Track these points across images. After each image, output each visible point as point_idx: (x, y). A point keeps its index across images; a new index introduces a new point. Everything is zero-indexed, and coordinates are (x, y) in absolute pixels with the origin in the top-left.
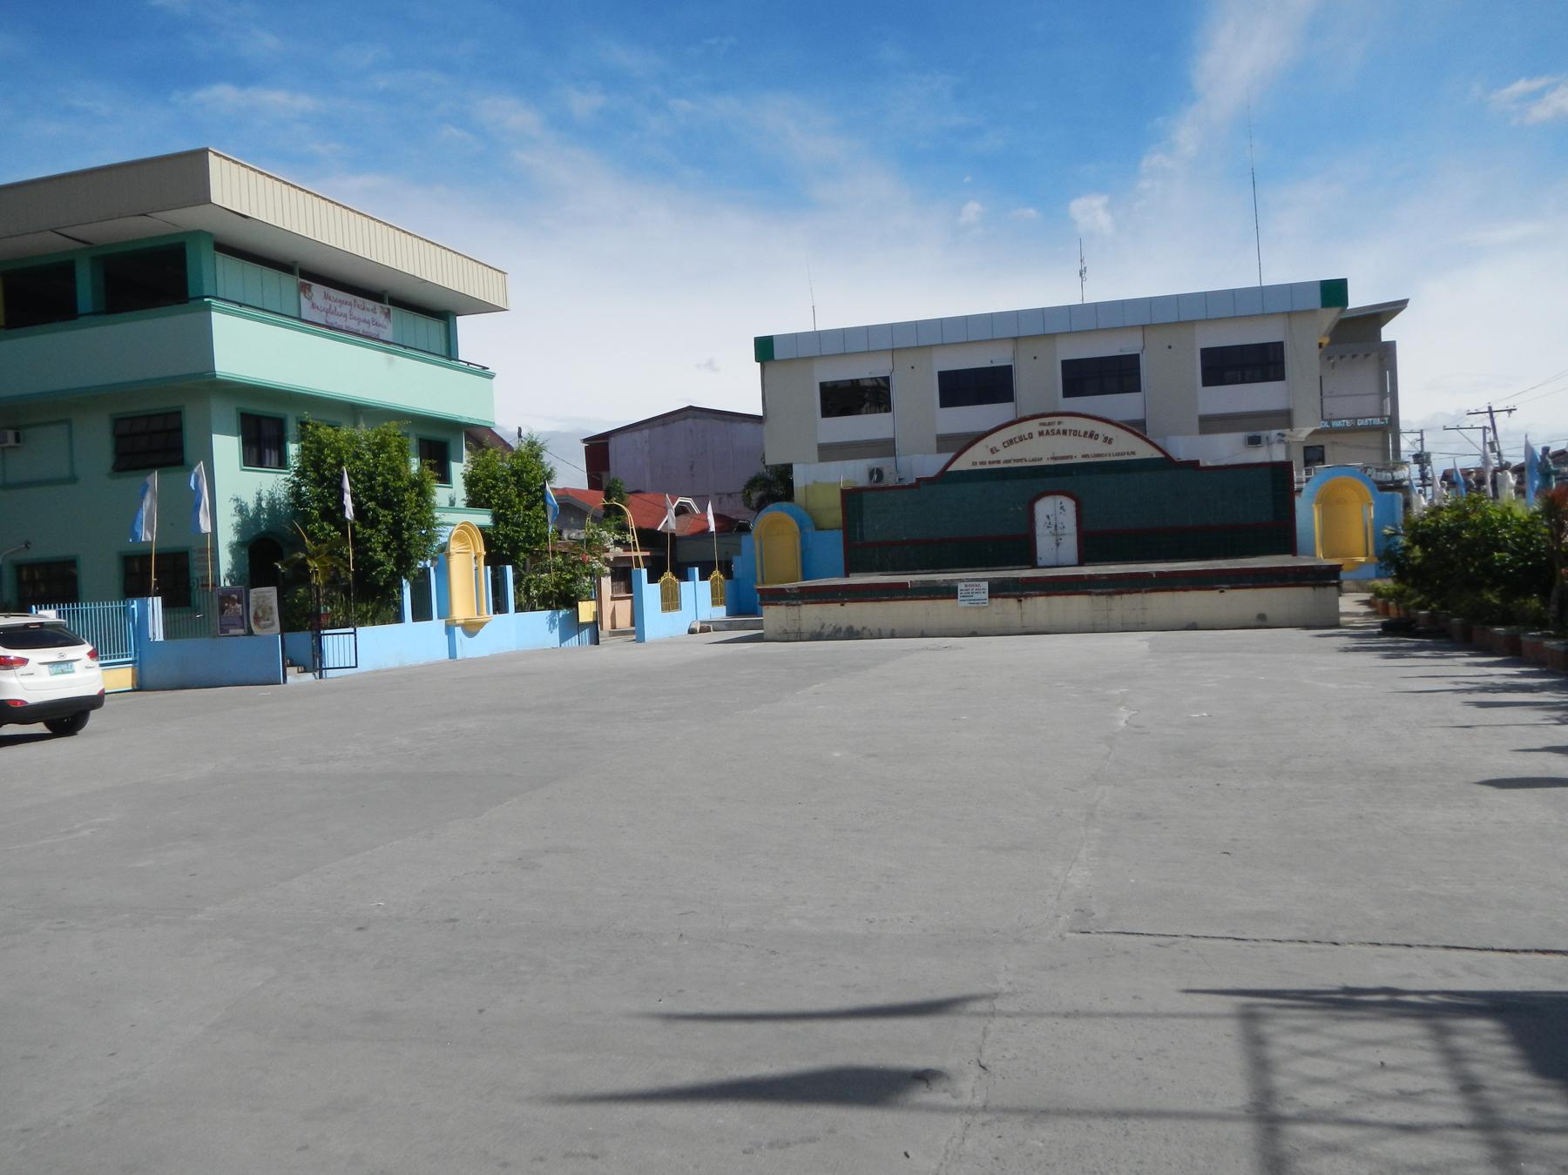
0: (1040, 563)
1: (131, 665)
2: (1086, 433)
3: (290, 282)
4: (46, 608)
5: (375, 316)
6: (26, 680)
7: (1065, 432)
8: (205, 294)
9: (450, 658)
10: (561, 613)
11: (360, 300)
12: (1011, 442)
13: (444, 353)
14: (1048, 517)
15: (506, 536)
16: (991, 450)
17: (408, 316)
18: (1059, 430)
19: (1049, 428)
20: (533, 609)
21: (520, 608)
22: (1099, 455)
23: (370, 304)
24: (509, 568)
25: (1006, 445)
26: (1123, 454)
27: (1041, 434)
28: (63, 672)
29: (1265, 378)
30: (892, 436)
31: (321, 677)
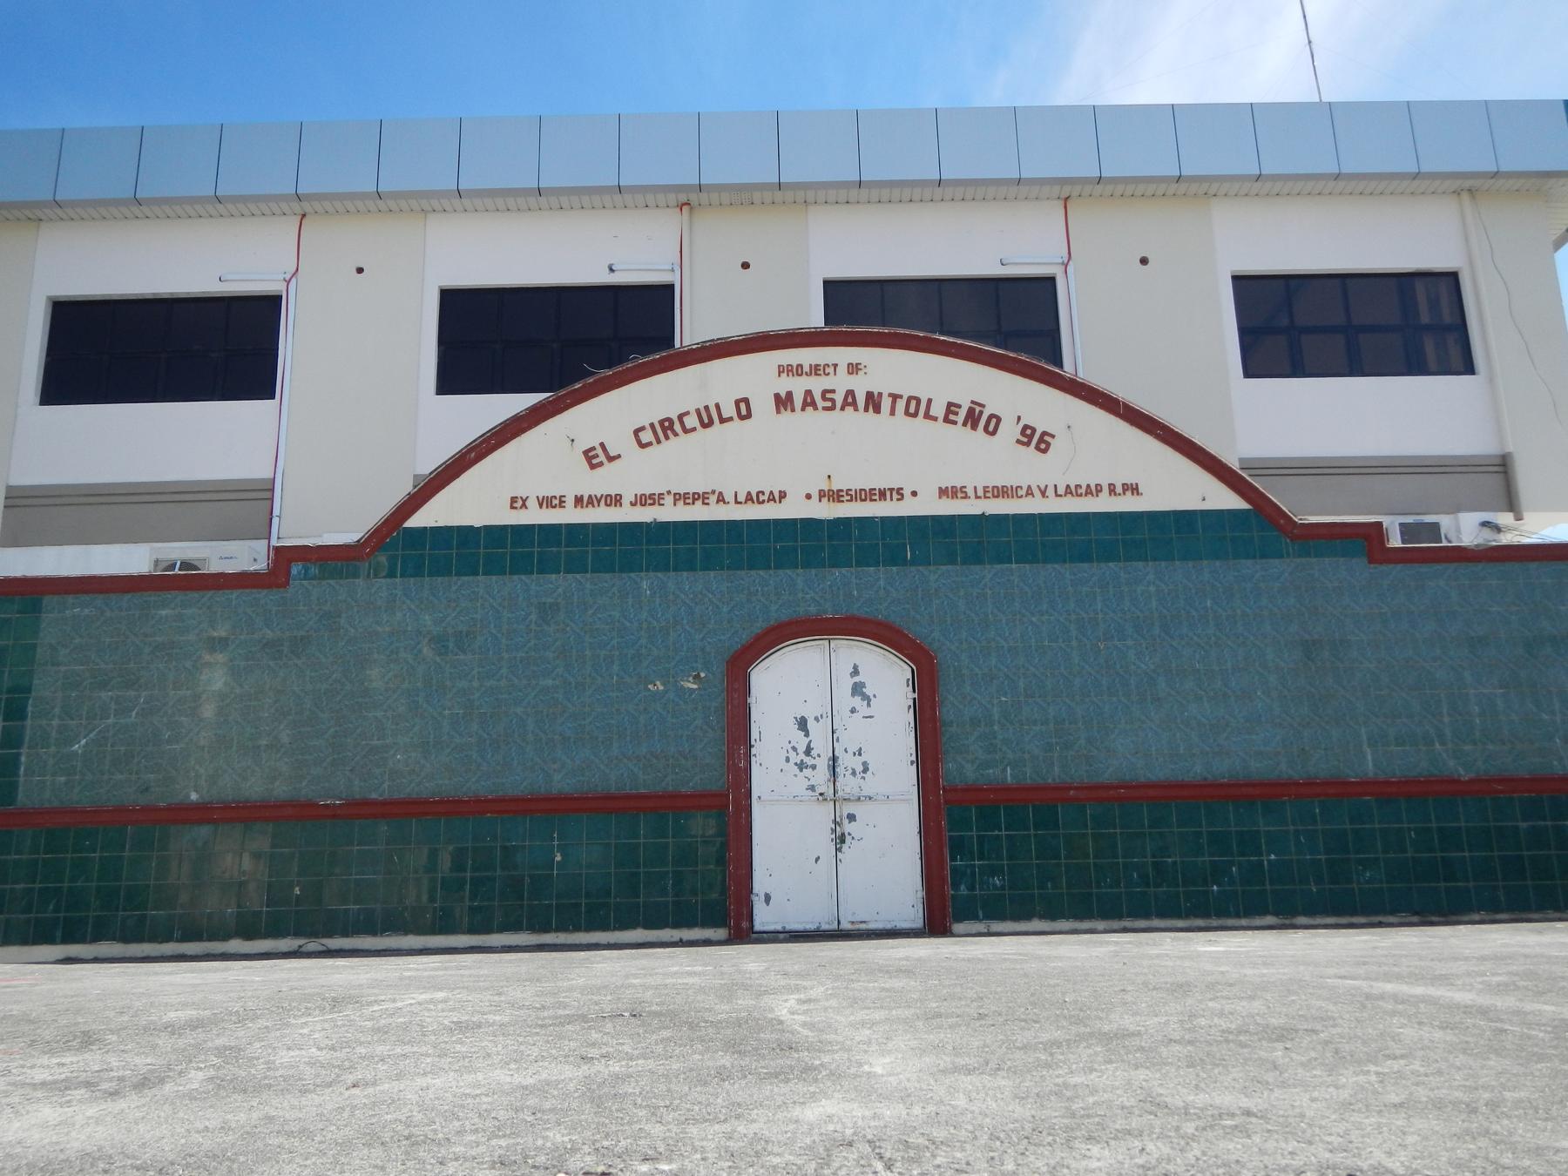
0: (764, 918)
2: (951, 408)
7: (873, 402)
12: (666, 428)
14: (802, 724)
16: (589, 455)
18: (850, 393)
19: (817, 385)
22: (1002, 492)
25: (647, 436)
26: (1093, 491)
27: (783, 402)
29: (1414, 365)
30: (268, 474)
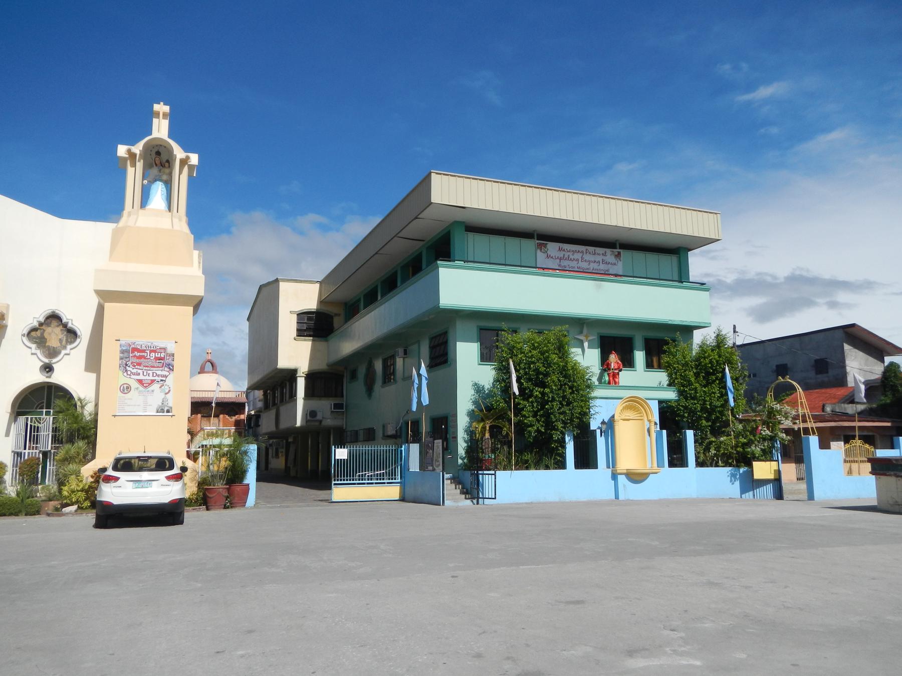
1: (399, 484)
3: (529, 245)
4: (341, 448)
5: (604, 258)
6: (115, 490)
8: (456, 259)
9: (615, 498)
10: (742, 470)
11: (591, 249)
13: (676, 277)
15: (686, 407)
17: (639, 256)
20: (717, 466)
21: (700, 464)
23: (600, 250)
24: (690, 434)
28: (142, 487)
31: (478, 503)
